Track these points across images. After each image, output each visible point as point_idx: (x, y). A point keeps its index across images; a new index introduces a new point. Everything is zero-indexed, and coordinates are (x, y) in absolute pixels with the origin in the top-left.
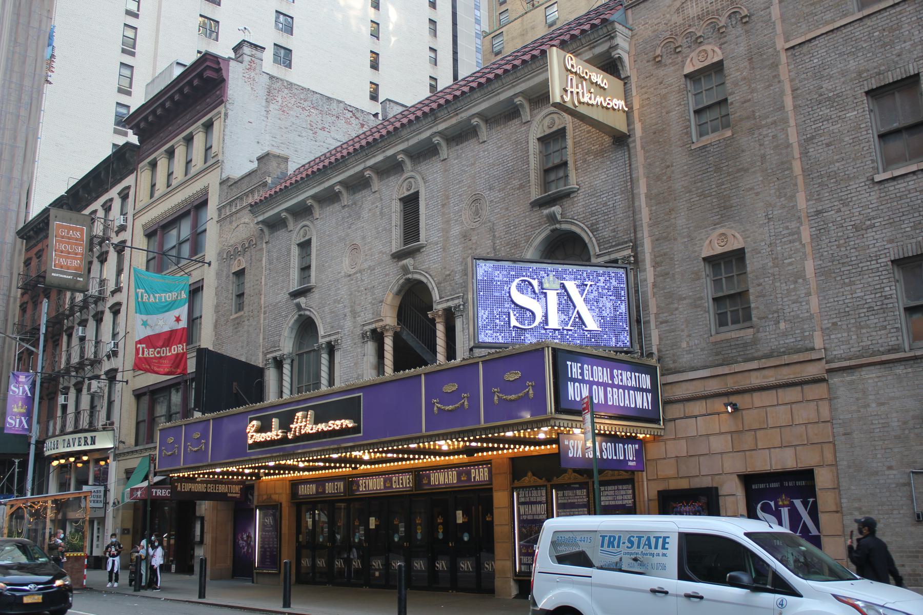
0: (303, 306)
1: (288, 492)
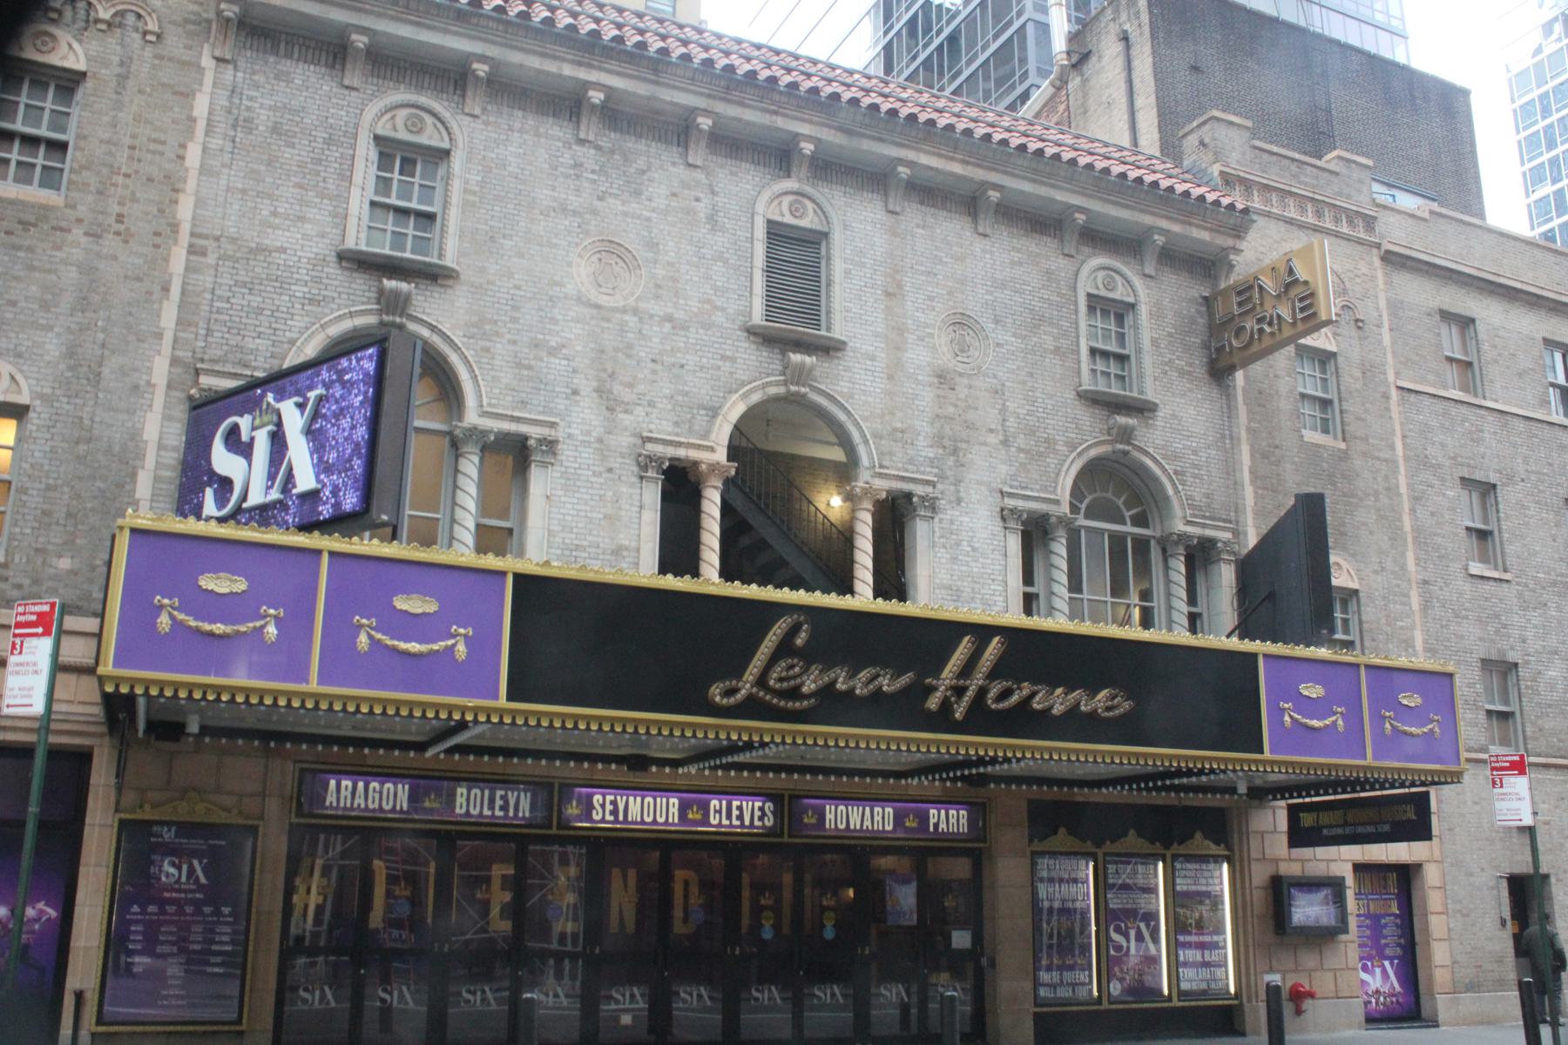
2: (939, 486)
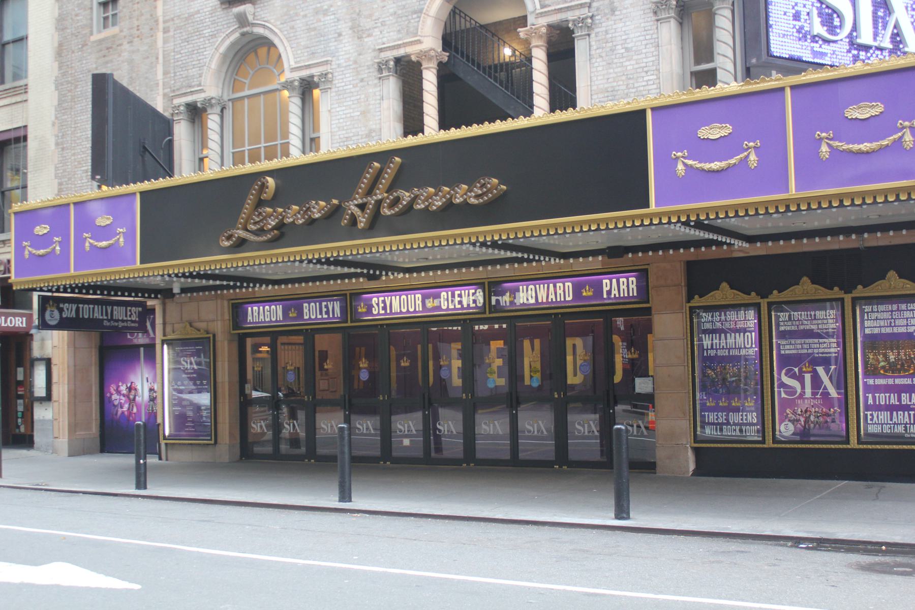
0: (250, 18)
1: (227, 317)
2: (595, 5)
